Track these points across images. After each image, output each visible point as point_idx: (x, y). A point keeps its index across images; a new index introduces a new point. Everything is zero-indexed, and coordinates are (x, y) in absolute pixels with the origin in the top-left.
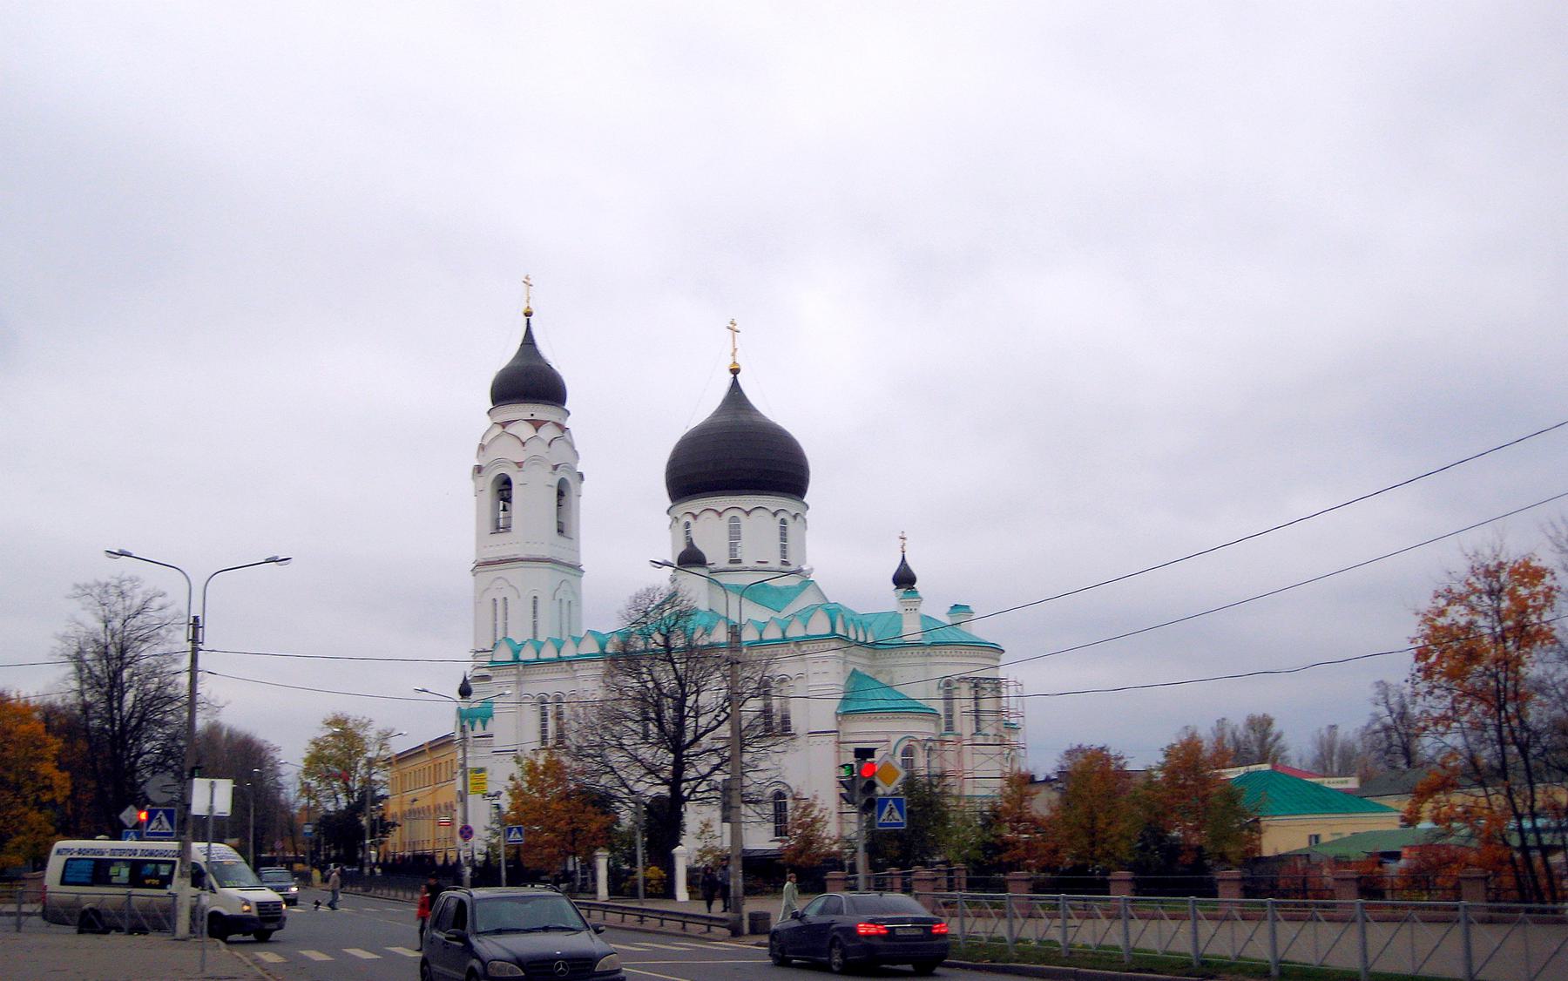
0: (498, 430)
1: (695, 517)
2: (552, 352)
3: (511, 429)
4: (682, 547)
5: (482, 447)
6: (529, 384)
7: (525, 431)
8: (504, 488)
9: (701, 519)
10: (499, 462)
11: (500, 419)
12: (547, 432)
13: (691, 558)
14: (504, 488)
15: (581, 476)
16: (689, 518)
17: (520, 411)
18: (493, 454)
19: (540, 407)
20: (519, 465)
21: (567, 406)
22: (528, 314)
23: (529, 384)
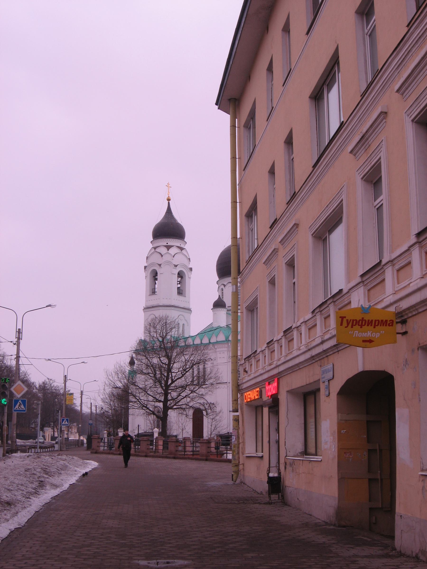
0: (153, 250)
1: (225, 286)
2: (179, 216)
3: (158, 250)
4: (216, 298)
5: (147, 258)
6: (169, 230)
7: (163, 250)
8: (155, 276)
9: (227, 287)
10: (152, 264)
11: (156, 245)
12: (173, 251)
13: (219, 304)
14: (155, 276)
15: (191, 269)
16: (223, 287)
17: (164, 242)
18: (151, 260)
19: (171, 239)
20: (160, 265)
21: (185, 240)
22: (169, 200)
23: (169, 230)
